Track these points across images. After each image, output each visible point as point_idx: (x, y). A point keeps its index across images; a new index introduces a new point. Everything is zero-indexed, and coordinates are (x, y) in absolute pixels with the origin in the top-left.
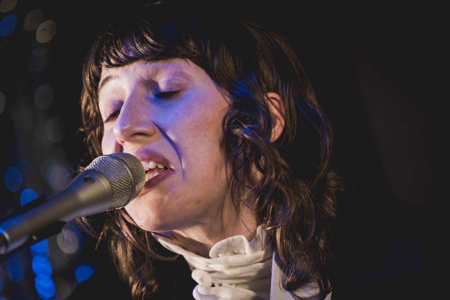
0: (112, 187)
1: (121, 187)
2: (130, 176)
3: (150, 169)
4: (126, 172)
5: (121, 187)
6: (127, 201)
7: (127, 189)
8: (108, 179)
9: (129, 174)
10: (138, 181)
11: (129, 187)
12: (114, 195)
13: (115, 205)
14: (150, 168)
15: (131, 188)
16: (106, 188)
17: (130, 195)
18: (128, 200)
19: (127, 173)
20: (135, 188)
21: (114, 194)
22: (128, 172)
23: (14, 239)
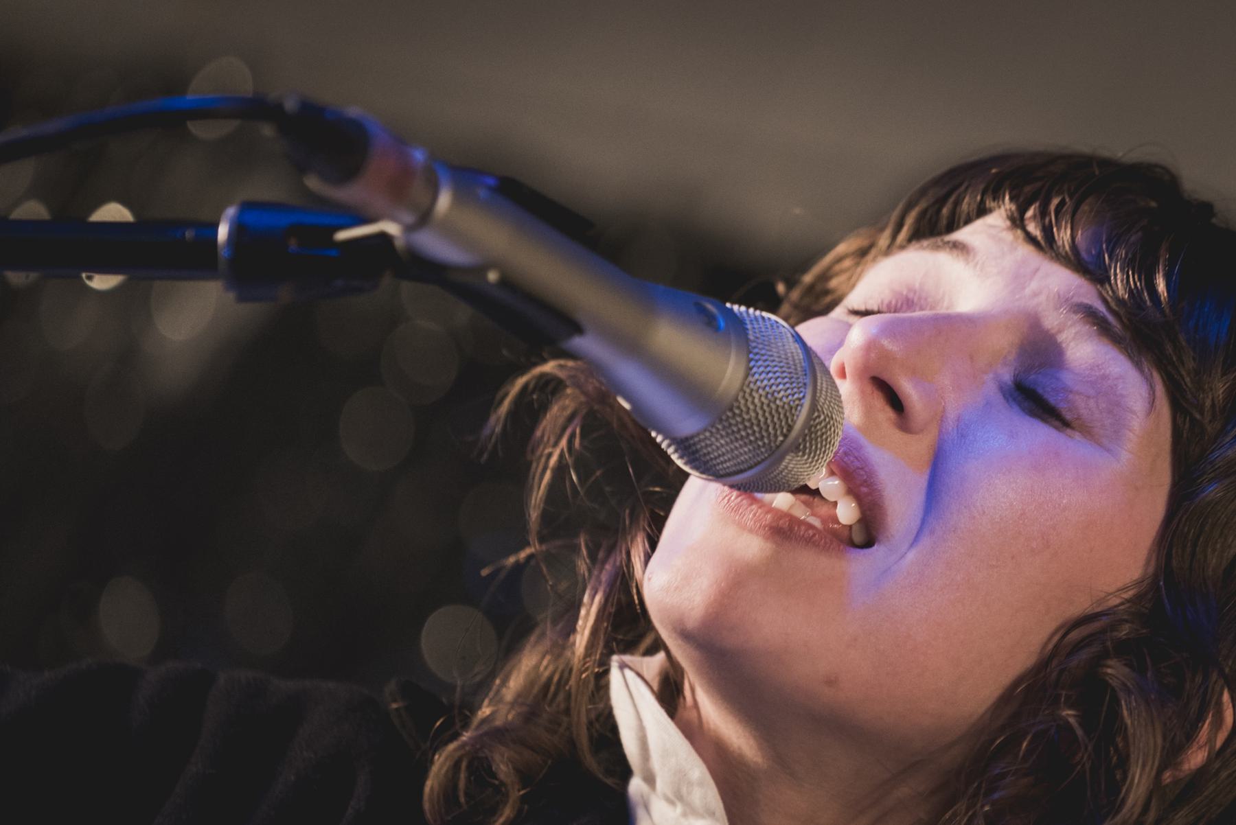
0: (737, 400)
1: (760, 412)
2: (800, 411)
3: (818, 489)
4: (801, 395)
5: (760, 412)
6: (738, 468)
7: (769, 434)
8: (750, 360)
9: (802, 405)
10: (805, 447)
11: (776, 436)
12: (730, 414)
13: (707, 446)
14: (820, 489)
15: (778, 443)
16: (725, 383)
17: (759, 459)
18: (742, 467)
19: (800, 399)
20: (782, 458)
21: (731, 410)
22: (804, 397)
23: (449, 231)
